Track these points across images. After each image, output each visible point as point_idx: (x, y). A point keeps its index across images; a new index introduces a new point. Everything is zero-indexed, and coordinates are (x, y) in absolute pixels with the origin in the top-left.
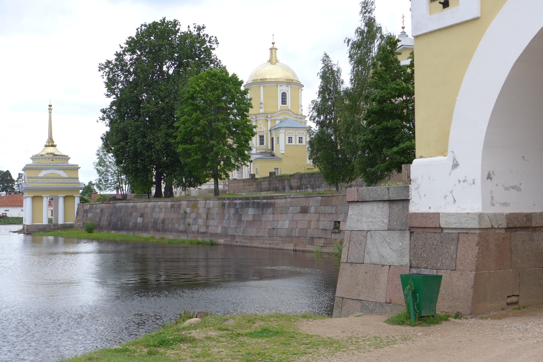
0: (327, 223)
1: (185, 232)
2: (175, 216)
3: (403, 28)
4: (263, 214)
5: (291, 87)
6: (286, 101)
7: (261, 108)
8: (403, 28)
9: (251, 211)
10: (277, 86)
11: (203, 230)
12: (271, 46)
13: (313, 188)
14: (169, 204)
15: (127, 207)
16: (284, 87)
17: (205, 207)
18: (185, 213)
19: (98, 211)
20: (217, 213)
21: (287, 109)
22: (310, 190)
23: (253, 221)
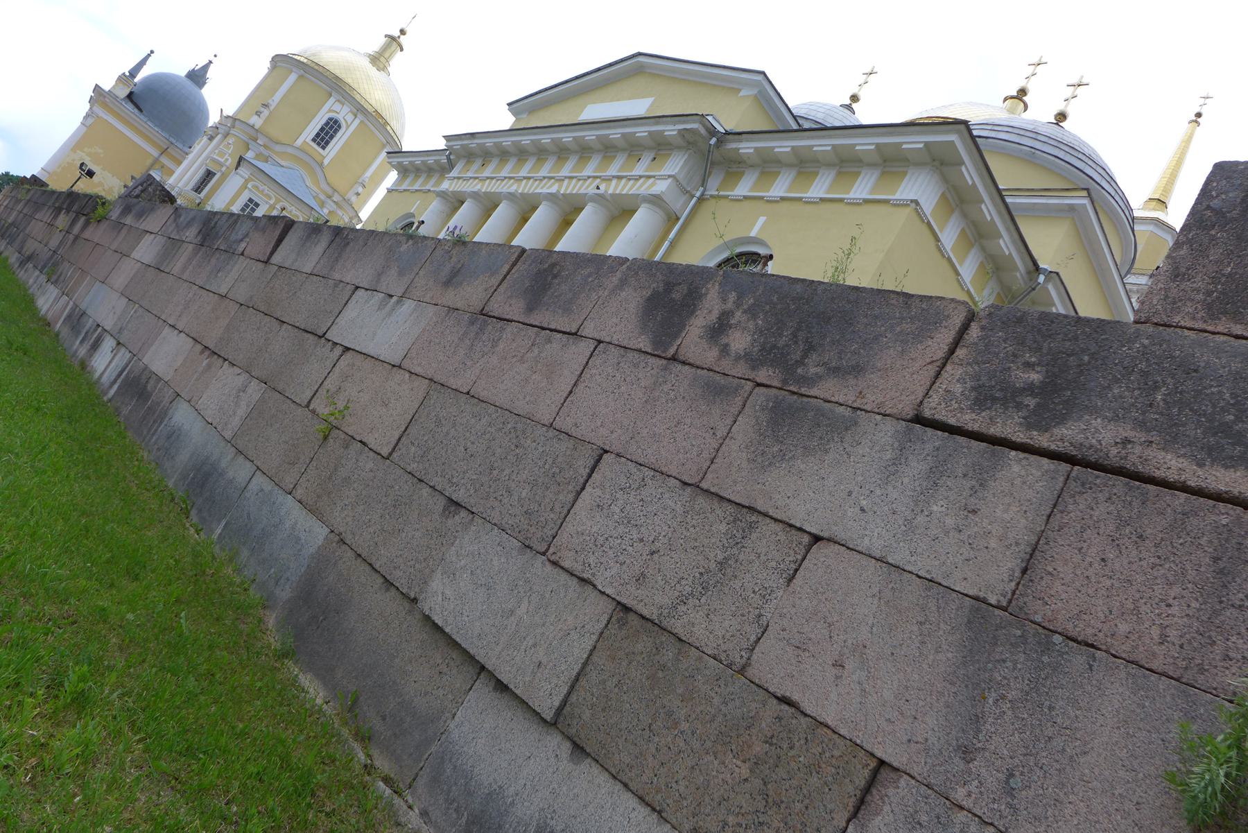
5: (362, 122)
6: (327, 143)
7: (258, 113)
10: (331, 95)
12: (396, 34)
16: (346, 109)
21: (318, 159)
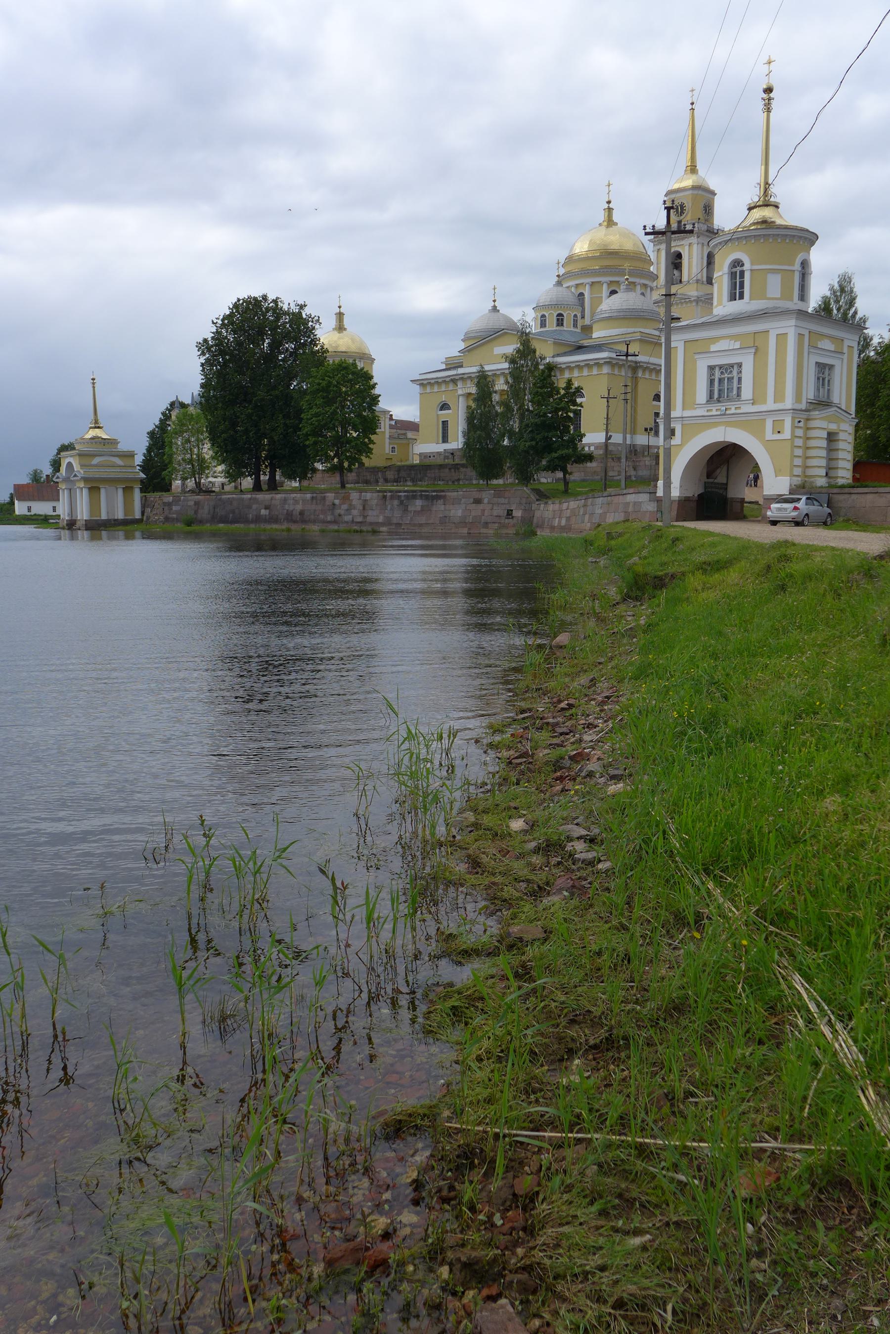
0: (500, 511)
1: (335, 522)
2: (320, 507)
3: (494, 301)
4: (432, 505)
8: (494, 301)
9: (419, 503)
11: (360, 519)
13: (413, 481)
14: (309, 496)
15: (243, 499)
17: (360, 499)
18: (334, 504)
19: (192, 503)
20: (377, 505)
22: (409, 483)
23: (422, 510)
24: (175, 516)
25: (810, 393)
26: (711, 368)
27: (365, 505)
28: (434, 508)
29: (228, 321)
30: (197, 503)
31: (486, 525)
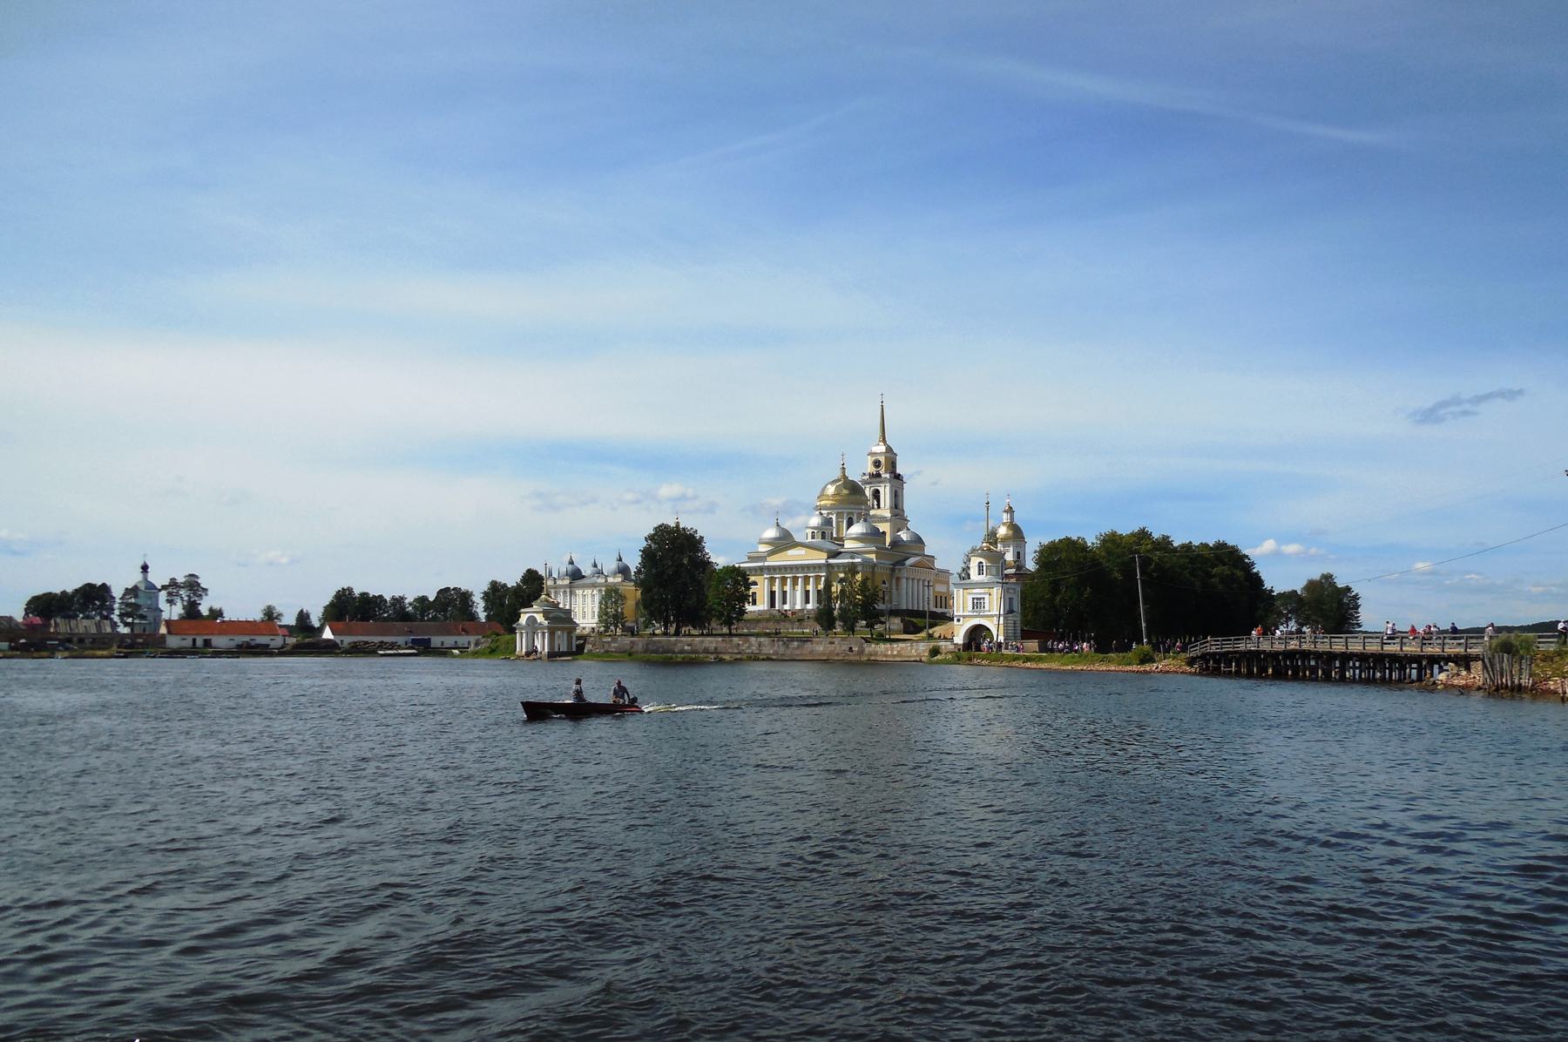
0: (846, 648)
1: (740, 653)
9: (796, 644)
24: (613, 650)
25: (1007, 608)
26: (973, 599)
27: (760, 644)
28: (806, 646)
29: (651, 538)
30: (631, 642)
31: (838, 654)
